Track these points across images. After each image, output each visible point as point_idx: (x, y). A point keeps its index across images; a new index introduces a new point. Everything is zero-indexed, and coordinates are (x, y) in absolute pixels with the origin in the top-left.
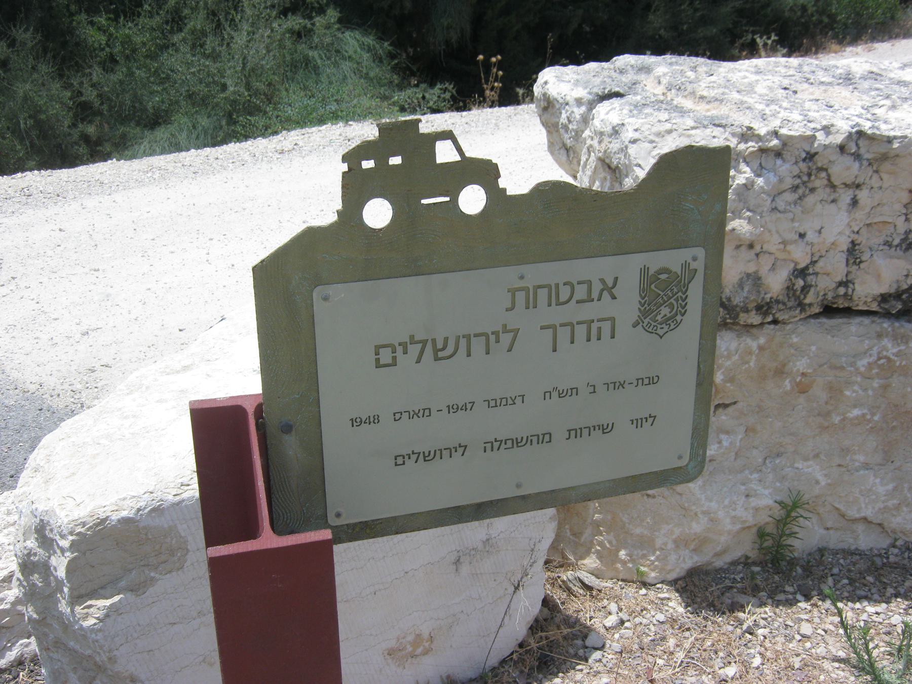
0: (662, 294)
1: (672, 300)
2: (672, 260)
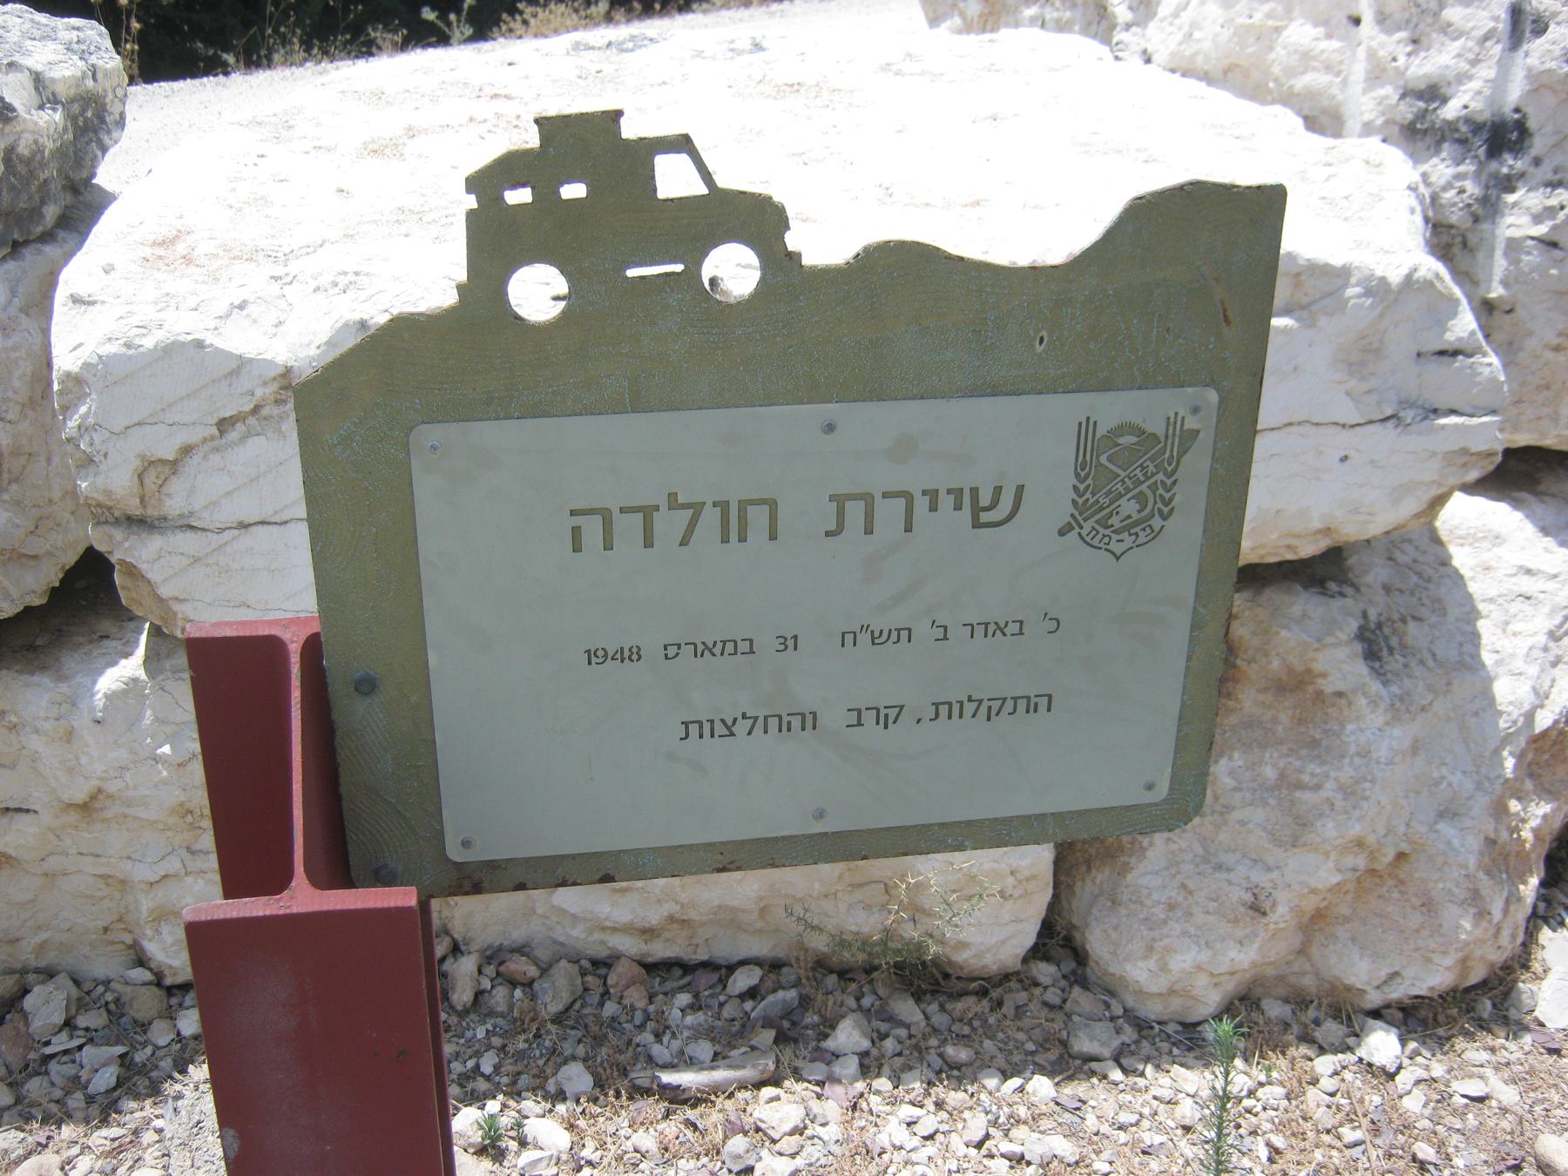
0: (1123, 474)
1: (1144, 487)
2: (1148, 408)
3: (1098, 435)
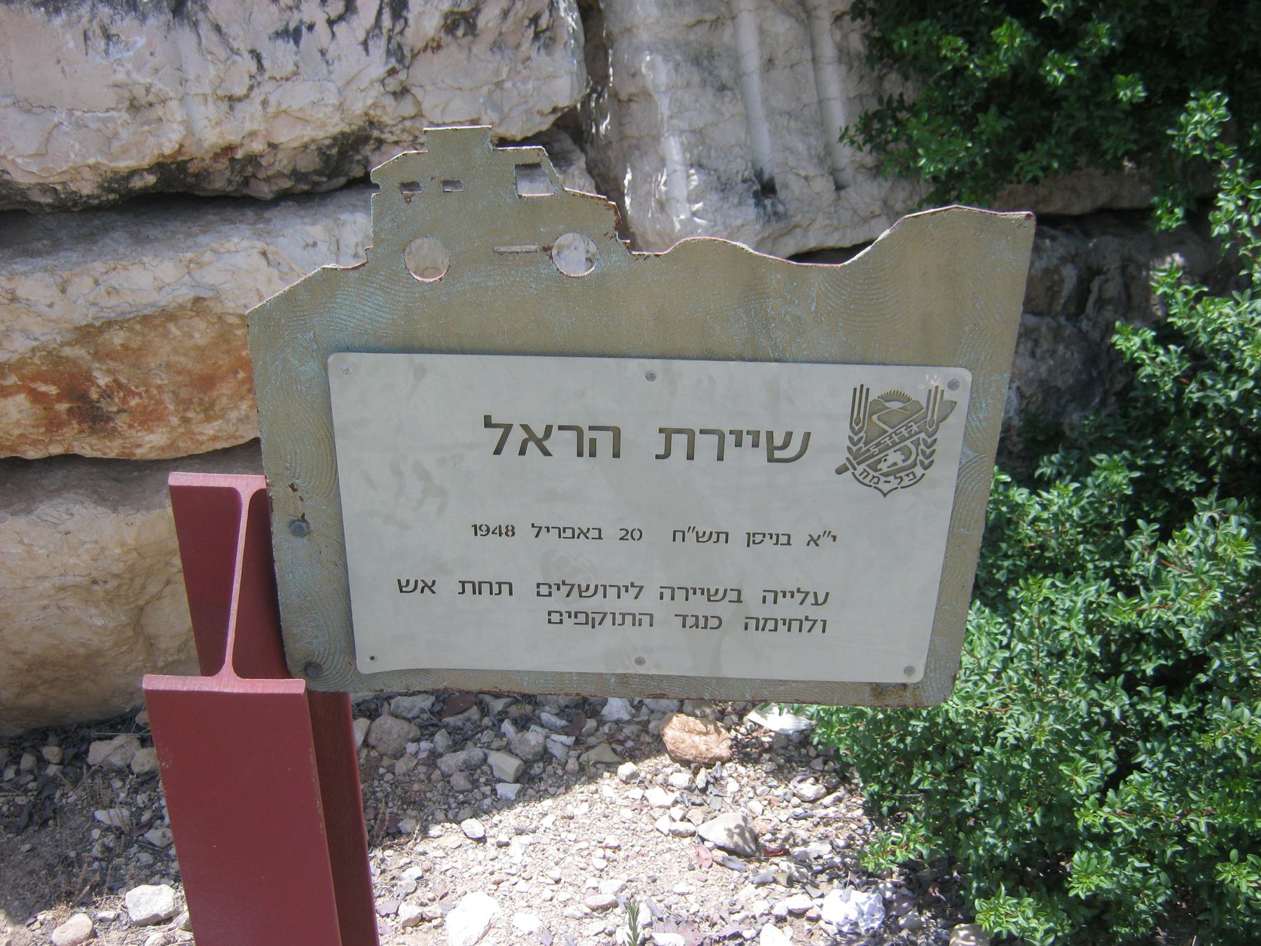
0: (890, 431)
1: (908, 443)
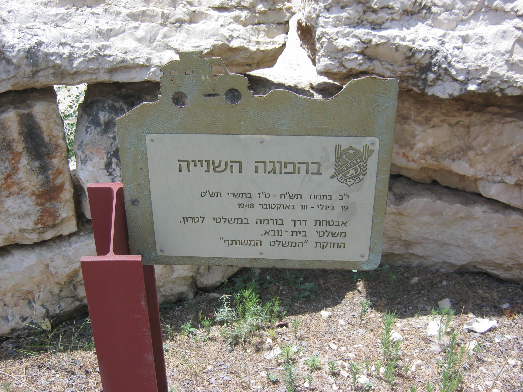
1: (357, 166)
2: (360, 143)
3: (342, 149)
